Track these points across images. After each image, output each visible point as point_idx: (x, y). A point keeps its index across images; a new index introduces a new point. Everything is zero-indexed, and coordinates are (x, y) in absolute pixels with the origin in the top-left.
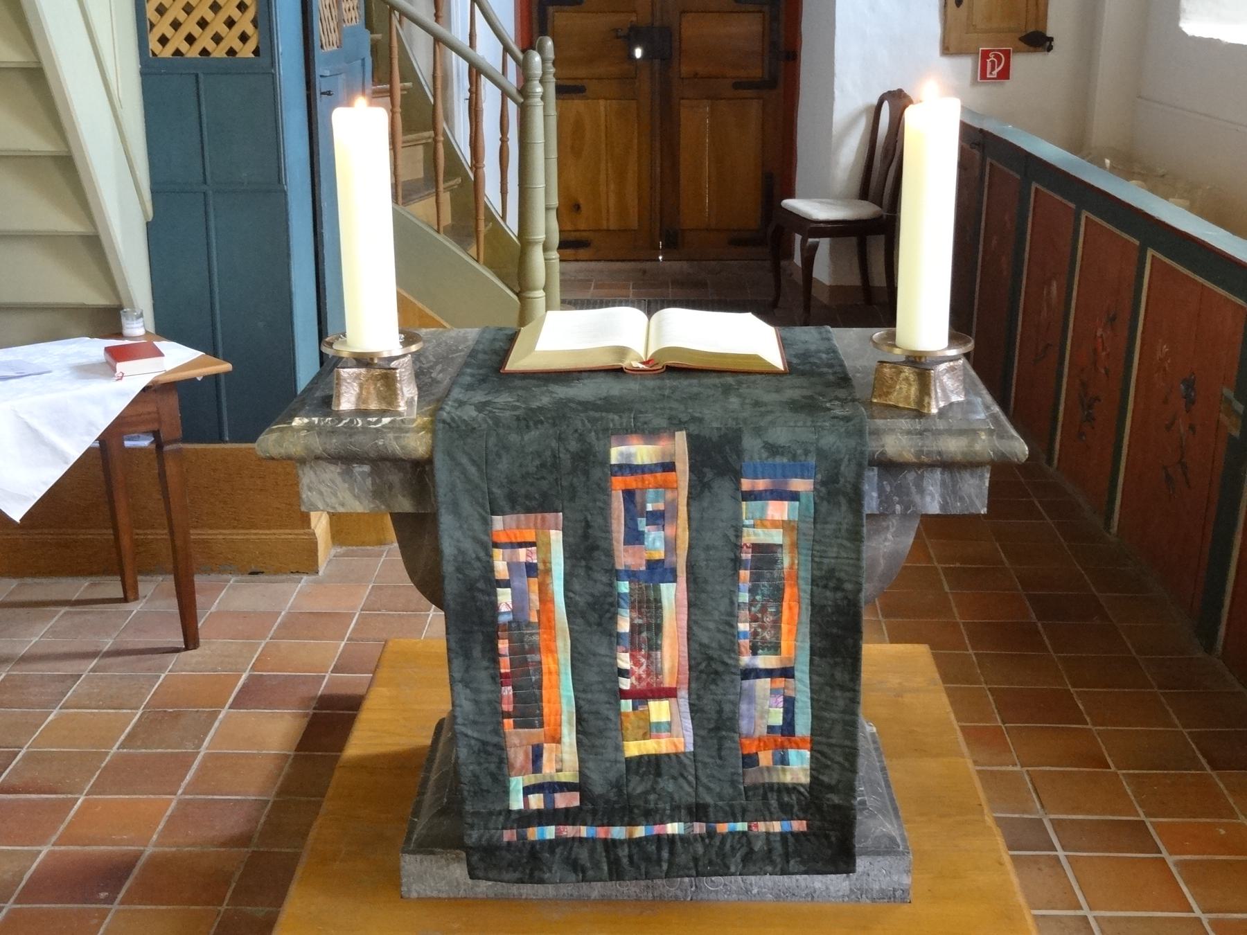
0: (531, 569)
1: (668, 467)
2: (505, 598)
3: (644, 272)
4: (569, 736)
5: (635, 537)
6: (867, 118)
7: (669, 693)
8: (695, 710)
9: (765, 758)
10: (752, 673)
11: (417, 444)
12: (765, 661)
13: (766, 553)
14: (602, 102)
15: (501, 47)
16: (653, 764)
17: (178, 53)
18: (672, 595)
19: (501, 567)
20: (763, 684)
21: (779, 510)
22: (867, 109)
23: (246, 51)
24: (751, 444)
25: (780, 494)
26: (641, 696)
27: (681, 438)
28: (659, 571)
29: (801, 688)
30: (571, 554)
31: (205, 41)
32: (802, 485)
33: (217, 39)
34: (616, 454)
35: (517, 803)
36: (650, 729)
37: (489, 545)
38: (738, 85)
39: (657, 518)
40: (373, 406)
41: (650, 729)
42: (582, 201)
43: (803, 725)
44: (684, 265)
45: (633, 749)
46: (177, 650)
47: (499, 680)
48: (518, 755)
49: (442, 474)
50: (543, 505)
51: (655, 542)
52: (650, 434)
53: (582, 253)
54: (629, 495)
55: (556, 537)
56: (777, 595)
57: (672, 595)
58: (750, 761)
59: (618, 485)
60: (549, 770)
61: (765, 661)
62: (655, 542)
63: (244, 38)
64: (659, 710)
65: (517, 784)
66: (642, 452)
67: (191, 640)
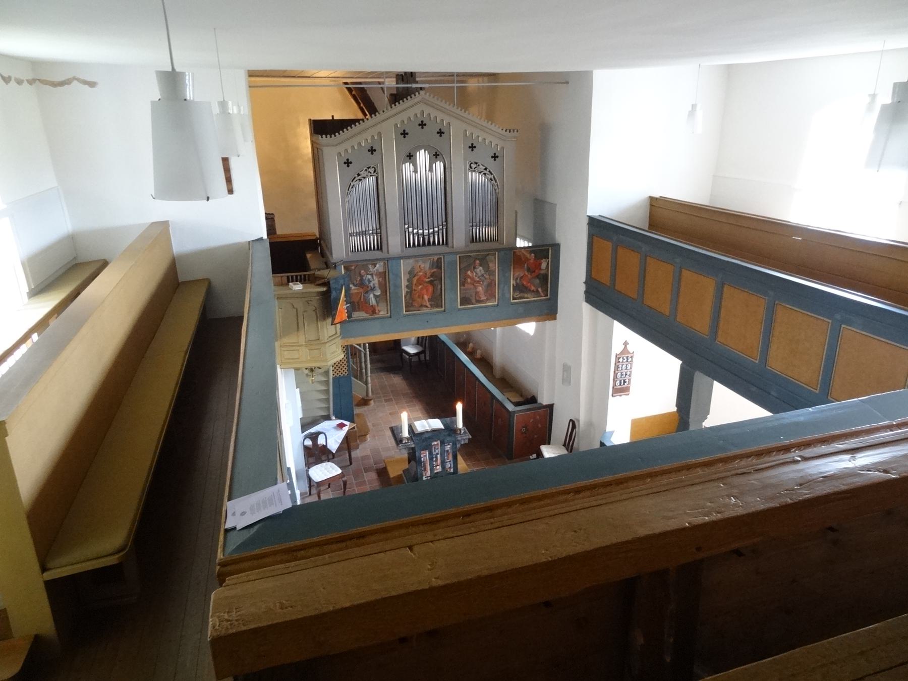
0: (425, 456)
1: (438, 444)
2: (422, 459)
4: (429, 471)
5: (435, 451)
7: (438, 466)
8: (441, 466)
9: (449, 470)
10: (447, 462)
11: (413, 446)
12: (448, 461)
13: (448, 451)
16: (438, 473)
17: (336, 376)
18: (439, 456)
19: (422, 456)
20: (448, 463)
21: (449, 446)
24: (446, 441)
25: (449, 445)
26: (436, 466)
27: (439, 442)
28: (437, 454)
29: (452, 462)
30: (429, 454)
31: (340, 374)
32: (450, 444)
33: (342, 373)
34: (433, 444)
35: (424, 479)
36: (437, 469)
37: (421, 454)
39: (437, 449)
40: (406, 442)
41: (437, 469)
43: (452, 466)
45: (436, 472)
46: (349, 466)
47: (422, 467)
48: (424, 474)
49: (416, 449)
50: (426, 450)
51: (437, 451)
52: (436, 441)
54: (435, 448)
55: (427, 453)
56: (449, 454)
57: (439, 456)
58: (447, 471)
60: (427, 475)
61: (448, 461)
62: (437, 451)
63: (346, 373)
64: (438, 467)
65: (424, 477)
66: (435, 443)
67: (351, 463)
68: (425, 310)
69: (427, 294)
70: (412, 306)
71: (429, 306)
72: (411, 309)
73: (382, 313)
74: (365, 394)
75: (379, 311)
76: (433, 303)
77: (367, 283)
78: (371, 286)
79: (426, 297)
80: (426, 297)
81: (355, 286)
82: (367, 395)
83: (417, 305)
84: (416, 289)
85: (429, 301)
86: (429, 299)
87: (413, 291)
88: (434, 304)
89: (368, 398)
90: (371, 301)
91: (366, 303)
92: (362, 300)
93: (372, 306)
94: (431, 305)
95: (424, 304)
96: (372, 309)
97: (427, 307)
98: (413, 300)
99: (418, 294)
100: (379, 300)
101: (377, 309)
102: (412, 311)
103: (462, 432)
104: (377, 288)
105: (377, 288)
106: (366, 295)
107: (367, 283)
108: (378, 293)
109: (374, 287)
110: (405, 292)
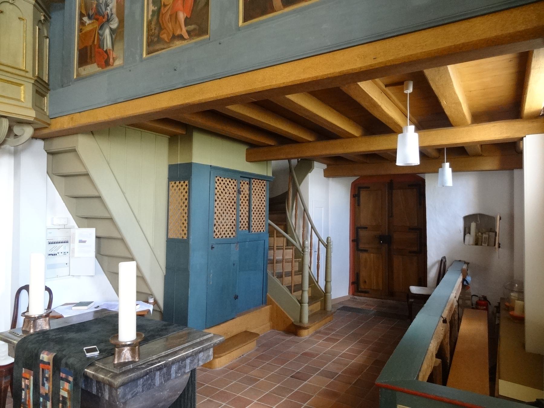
3: (383, 302)
6: (438, 264)
14: (372, 254)
15: (318, 239)
22: (438, 262)
23: (185, 237)
38: (410, 252)
42: (366, 280)
44: (394, 302)
53: (366, 295)
59: (41, 366)
68: (178, 44)
69: (184, 11)
70: (160, 40)
71: (186, 36)
72: (158, 47)
73: (118, 63)
74: (298, 319)
75: (114, 59)
76: (192, 27)
77: (104, 10)
78: (108, 15)
79: (182, 16)
80: (182, 16)
81: (90, 18)
82: (301, 320)
83: (166, 39)
84: (166, 3)
85: (186, 25)
86: (186, 19)
87: (162, 8)
88: (194, 30)
89: (298, 324)
90: (105, 43)
91: (99, 47)
92: (96, 42)
93: (106, 52)
94: (189, 32)
95: (178, 32)
96: (106, 57)
97: (181, 37)
98: (161, 29)
99: (168, 16)
100: (116, 38)
101: (111, 52)
102: (157, 51)
103: (126, 355)
104: (114, 16)
105: (114, 16)
106: (101, 32)
107: (104, 10)
108: (114, 25)
109: (112, 14)
110: (150, 13)
